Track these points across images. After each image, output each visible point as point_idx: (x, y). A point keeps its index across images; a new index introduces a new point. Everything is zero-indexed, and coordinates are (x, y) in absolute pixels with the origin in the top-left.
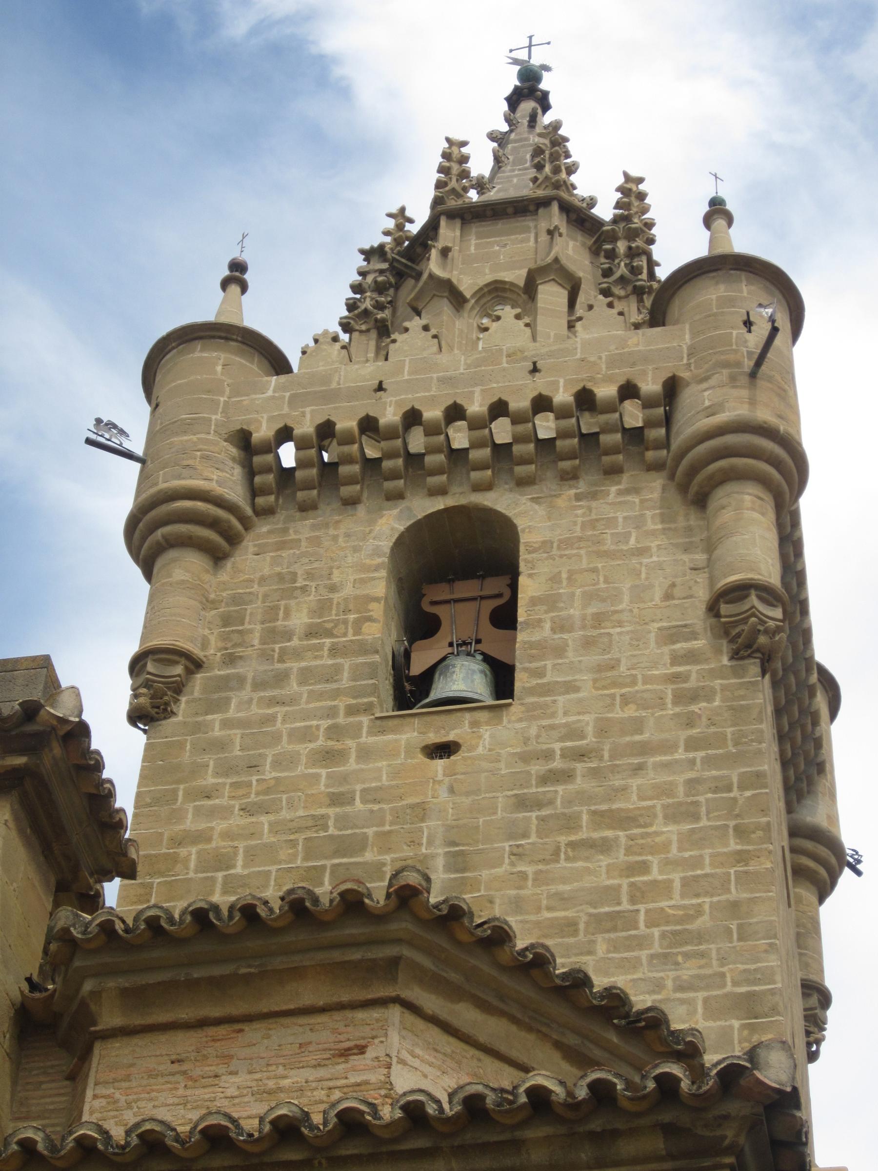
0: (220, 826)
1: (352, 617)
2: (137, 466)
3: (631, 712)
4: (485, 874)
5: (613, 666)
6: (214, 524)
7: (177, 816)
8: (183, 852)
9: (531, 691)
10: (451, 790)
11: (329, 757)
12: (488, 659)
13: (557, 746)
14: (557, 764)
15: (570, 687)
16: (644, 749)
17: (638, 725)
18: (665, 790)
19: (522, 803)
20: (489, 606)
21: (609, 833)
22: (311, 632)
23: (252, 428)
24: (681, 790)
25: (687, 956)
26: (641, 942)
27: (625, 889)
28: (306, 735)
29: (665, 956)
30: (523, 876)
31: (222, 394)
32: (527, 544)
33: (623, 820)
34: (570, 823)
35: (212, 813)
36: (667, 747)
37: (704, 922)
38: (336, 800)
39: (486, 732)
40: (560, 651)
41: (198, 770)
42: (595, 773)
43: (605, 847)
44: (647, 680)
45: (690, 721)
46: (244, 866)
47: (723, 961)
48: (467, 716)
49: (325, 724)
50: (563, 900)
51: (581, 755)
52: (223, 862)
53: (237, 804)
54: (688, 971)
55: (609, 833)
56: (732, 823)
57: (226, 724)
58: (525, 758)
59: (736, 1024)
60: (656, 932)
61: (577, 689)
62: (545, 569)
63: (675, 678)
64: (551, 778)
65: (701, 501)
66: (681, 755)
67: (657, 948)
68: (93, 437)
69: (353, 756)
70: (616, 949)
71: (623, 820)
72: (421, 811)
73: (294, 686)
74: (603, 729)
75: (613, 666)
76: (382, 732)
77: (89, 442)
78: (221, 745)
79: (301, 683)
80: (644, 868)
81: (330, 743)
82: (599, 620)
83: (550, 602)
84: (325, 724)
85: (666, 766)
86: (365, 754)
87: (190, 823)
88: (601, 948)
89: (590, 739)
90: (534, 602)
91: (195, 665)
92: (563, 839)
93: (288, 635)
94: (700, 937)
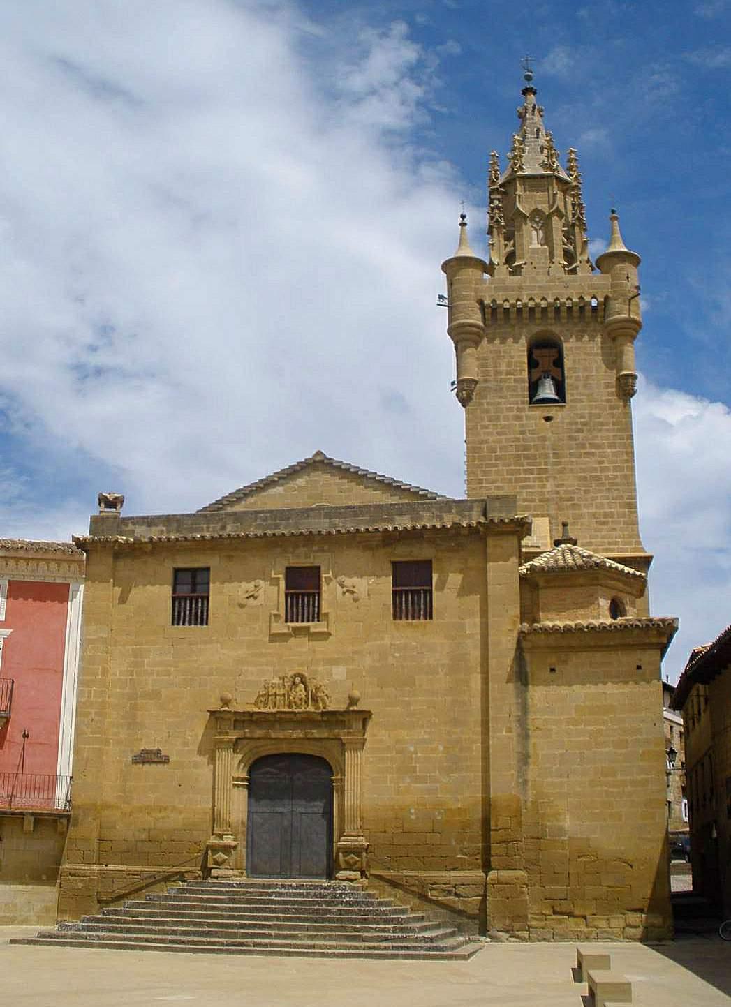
0: (491, 439)
1: (518, 369)
2: (447, 308)
3: (597, 412)
4: (563, 460)
5: (592, 394)
6: (475, 333)
7: (478, 434)
8: (482, 446)
9: (571, 401)
10: (552, 433)
11: (518, 418)
12: (553, 379)
13: (579, 420)
14: (580, 427)
15: (581, 401)
16: (602, 424)
17: (599, 416)
18: (607, 438)
19: (571, 438)
20: (552, 359)
21: (593, 450)
22: (508, 373)
23: (483, 299)
24: (611, 438)
25: (615, 490)
26: (603, 484)
27: (599, 468)
28: (510, 410)
29: (608, 489)
30: (572, 462)
31: (472, 283)
32: (566, 347)
33: (598, 447)
34: (583, 446)
35: (489, 434)
36: (607, 424)
37: (618, 480)
38: (523, 432)
39: (560, 413)
40: (577, 388)
41: (482, 419)
42: (589, 431)
43: (593, 454)
44: (602, 401)
45: (613, 416)
46: (500, 452)
47: (623, 492)
48: (555, 408)
49: (516, 406)
50: (583, 471)
51: (585, 424)
52: (493, 450)
53: (495, 432)
54: (616, 494)
55: (593, 450)
56: (625, 450)
57: (488, 404)
58: (571, 424)
59: (627, 510)
60: (607, 482)
61: (583, 402)
62: (571, 357)
63: (608, 401)
64: (578, 431)
65: (614, 339)
66: (611, 427)
67: (608, 487)
68: (439, 303)
69: (524, 418)
70: (598, 486)
71: (598, 447)
72: (544, 439)
73: (505, 393)
74: (591, 415)
75: (592, 394)
76: (532, 411)
77: (438, 305)
78: (487, 411)
79: (508, 391)
80: (603, 462)
81: (518, 413)
82: (588, 377)
83: (573, 370)
84: (516, 406)
85: (608, 430)
86: (528, 418)
87: (482, 437)
88: (593, 485)
89: (587, 420)
90: (569, 369)
91: (476, 382)
92: (582, 451)
93: (501, 373)
94: (617, 484)
